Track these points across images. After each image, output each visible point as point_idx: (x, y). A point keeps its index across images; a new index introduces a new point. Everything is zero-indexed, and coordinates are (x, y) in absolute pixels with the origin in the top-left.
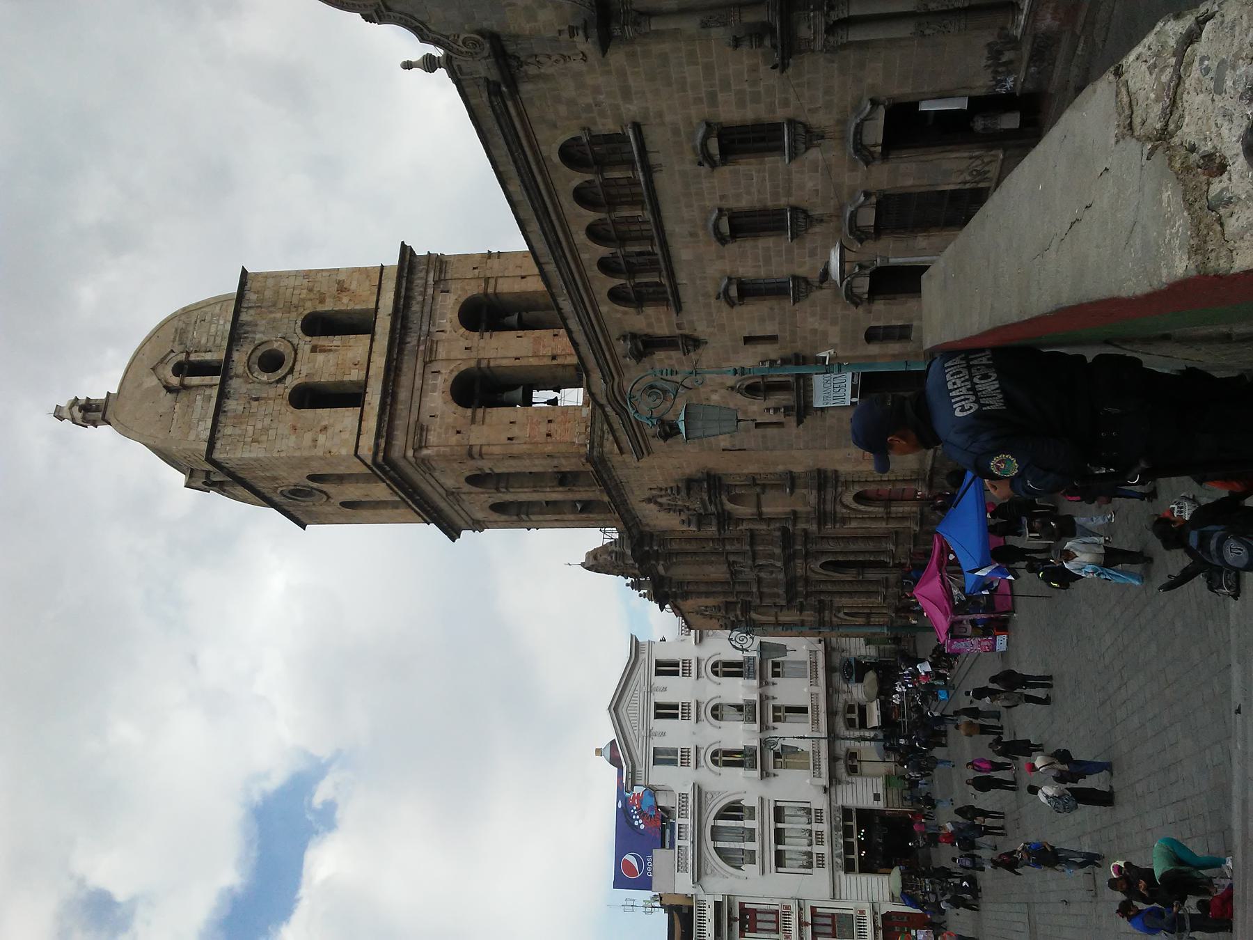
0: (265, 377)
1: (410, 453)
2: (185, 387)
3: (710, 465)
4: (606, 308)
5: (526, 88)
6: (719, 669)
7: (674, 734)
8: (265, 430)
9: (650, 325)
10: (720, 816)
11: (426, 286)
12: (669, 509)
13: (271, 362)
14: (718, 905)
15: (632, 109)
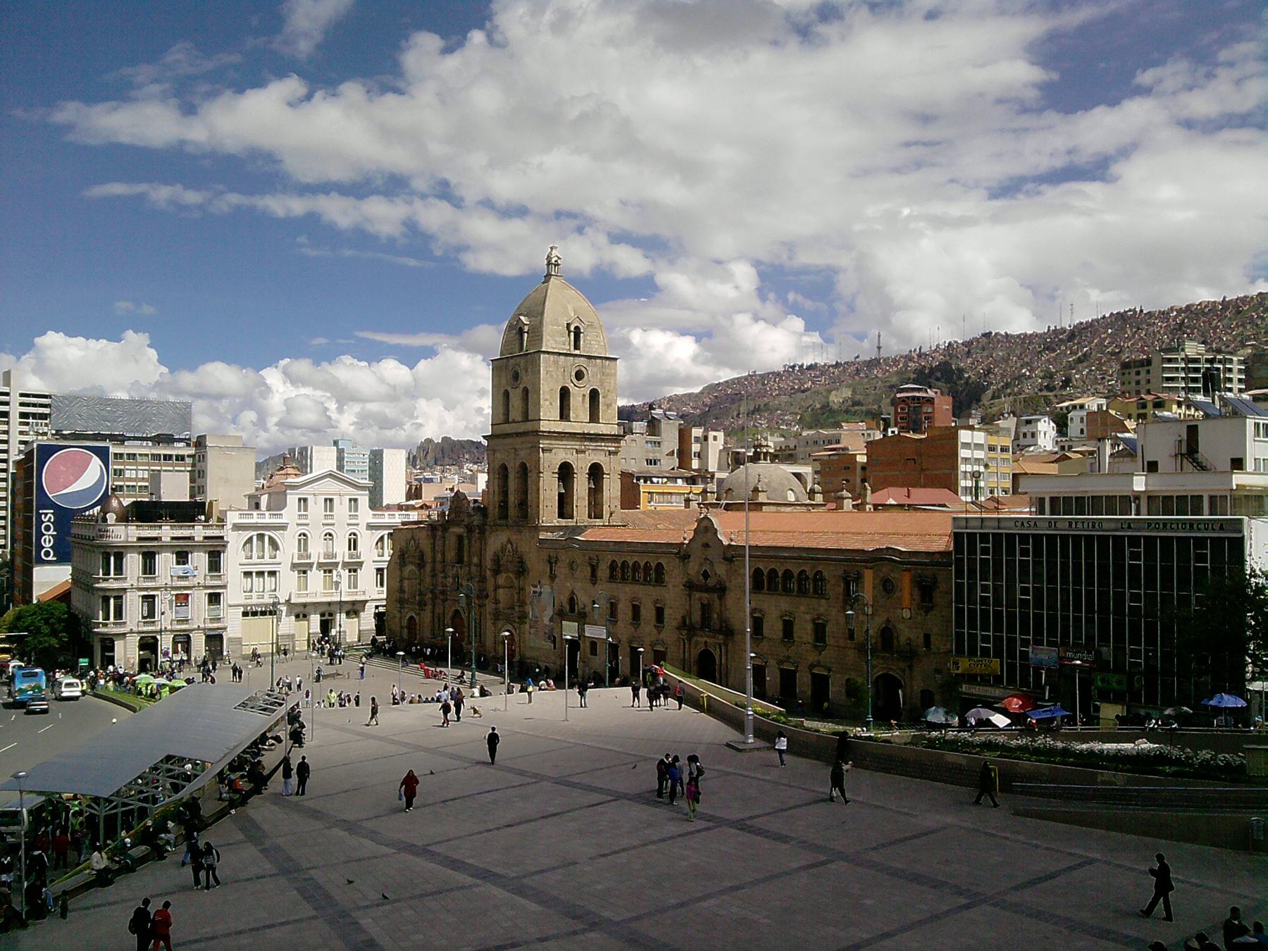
0: (573, 374)
1: (541, 446)
2: (570, 332)
3: (531, 573)
4: (609, 558)
5: (677, 560)
6: (352, 536)
7: (316, 508)
8: (552, 376)
9: (602, 570)
10: (270, 538)
11: (608, 447)
12: (503, 550)
13: (579, 376)
14: (222, 538)
15: (670, 586)
